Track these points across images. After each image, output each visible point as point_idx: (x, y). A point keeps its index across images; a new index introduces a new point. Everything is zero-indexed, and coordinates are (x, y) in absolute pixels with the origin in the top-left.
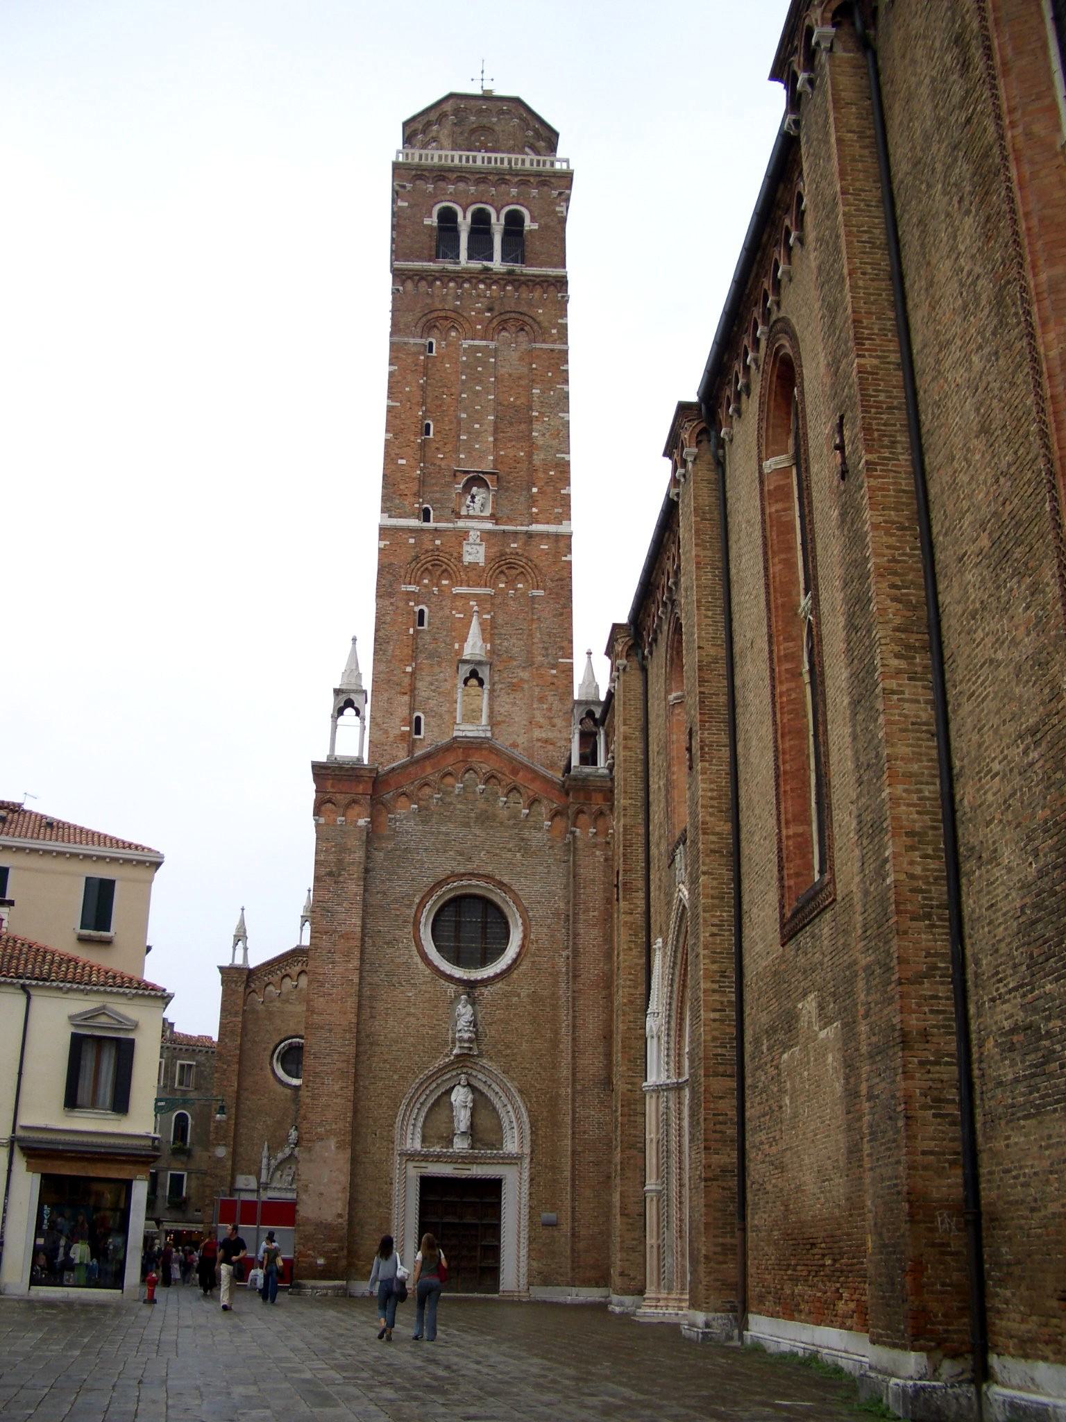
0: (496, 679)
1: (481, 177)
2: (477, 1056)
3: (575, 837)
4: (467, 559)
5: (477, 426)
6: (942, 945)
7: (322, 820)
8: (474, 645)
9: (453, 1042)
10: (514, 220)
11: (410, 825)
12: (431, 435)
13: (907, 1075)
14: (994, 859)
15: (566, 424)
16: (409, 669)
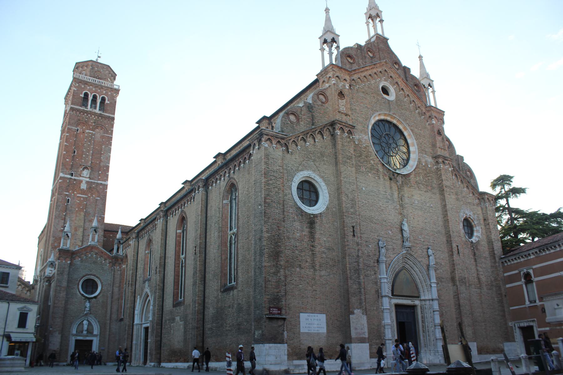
0: (86, 218)
1: (96, 86)
2: (90, 314)
3: (114, 268)
4: (82, 187)
5: (88, 153)
6: (202, 317)
7: (60, 261)
8: (95, 224)
9: (85, 311)
10: (103, 99)
11: (79, 263)
12: (76, 154)
13: (197, 332)
14: (209, 309)
15: (110, 156)
16: (64, 214)
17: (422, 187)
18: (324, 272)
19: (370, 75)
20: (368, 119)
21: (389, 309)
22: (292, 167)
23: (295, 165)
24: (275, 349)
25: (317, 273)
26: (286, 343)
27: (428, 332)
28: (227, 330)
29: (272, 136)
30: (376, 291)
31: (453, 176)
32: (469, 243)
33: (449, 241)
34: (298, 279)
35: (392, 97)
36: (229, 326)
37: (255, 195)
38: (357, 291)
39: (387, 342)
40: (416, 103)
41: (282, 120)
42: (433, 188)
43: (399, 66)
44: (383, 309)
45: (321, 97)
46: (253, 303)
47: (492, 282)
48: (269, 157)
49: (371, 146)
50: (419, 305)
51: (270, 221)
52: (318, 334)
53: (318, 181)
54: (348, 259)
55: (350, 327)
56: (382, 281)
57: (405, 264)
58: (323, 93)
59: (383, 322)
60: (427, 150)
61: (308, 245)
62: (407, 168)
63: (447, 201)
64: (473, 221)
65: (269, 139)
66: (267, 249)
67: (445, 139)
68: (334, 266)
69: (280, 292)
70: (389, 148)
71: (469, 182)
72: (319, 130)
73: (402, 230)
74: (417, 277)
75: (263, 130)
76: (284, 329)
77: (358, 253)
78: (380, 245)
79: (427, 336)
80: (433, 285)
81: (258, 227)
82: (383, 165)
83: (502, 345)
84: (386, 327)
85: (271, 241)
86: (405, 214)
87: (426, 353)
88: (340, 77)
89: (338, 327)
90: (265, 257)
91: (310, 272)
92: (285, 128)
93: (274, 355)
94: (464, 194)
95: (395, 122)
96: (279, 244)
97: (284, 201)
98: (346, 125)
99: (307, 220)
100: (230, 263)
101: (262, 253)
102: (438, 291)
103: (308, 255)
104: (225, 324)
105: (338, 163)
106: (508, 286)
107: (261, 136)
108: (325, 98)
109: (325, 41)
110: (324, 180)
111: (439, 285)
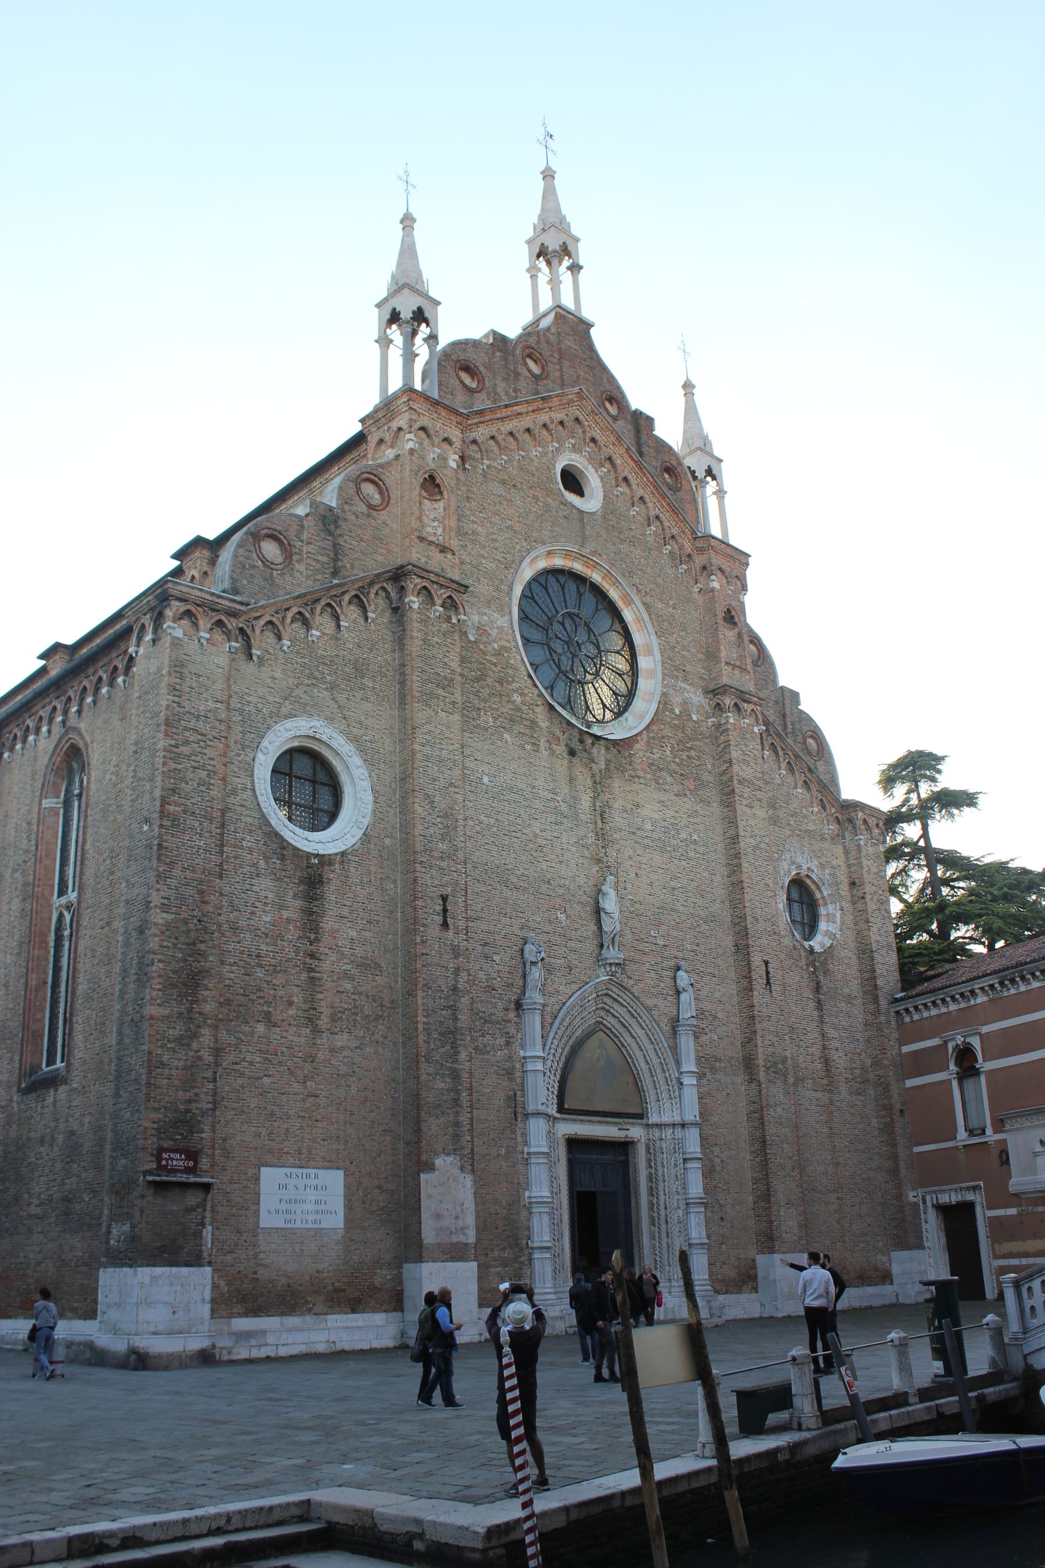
17: (669, 779)
18: (345, 1036)
19: (528, 430)
20: (512, 565)
21: (547, 1154)
22: (260, 706)
23: (271, 699)
24: (171, 1284)
25: (323, 1040)
26: (210, 1264)
27: (667, 1223)
28: (30, 1216)
29: (198, 605)
30: (509, 1098)
31: (763, 749)
32: (803, 953)
33: (742, 949)
34: (258, 1059)
35: (592, 502)
36: (38, 1202)
37: (133, 789)
38: (445, 1098)
39: (537, 1255)
40: (666, 524)
41: (235, 556)
42: (702, 784)
43: (619, 409)
44: (529, 1154)
45: (368, 489)
46: (109, 1135)
47: (863, 1068)
48: (185, 671)
49: (517, 647)
51: (177, 872)
52: (318, 1233)
53: (340, 750)
54: (423, 998)
55: (418, 1210)
56: (530, 1067)
57: (602, 1013)
58: (373, 478)
59: (527, 1194)
60: (688, 668)
61: (297, 951)
62: (627, 719)
63: (741, 824)
64: (819, 888)
65: (188, 613)
66: (160, 961)
67: (746, 639)
68: (378, 1018)
69: (196, 1101)
70: (574, 656)
71: (810, 770)
72: (353, 593)
73: (598, 911)
74: (639, 1055)
75: (170, 585)
76: (204, 1217)
77: (456, 981)
78: (526, 955)
79: (664, 1234)
80: (689, 1080)
81: (136, 892)
82: (552, 708)
83: (884, 1259)
85: (176, 938)
86: (612, 862)
88: (432, 432)
89: (382, 1209)
90: (154, 990)
91: (297, 1038)
92: (245, 582)
93: (165, 1303)
94: (795, 805)
95: (596, 577)
96: (202, 946)
97: (223, 812)
98: (442, 581)
99: (299, 874)
100: (52, 998)
101: (146, 974)
102: (700, 1098)
103: (296, 982)
104: (26, 1196)
105: (408, 697)
106: (910, 1083)
107: (163, 601)
108: (381, 493)
109: (394, 318)
110: (362, 751)
111: (704, 1081)
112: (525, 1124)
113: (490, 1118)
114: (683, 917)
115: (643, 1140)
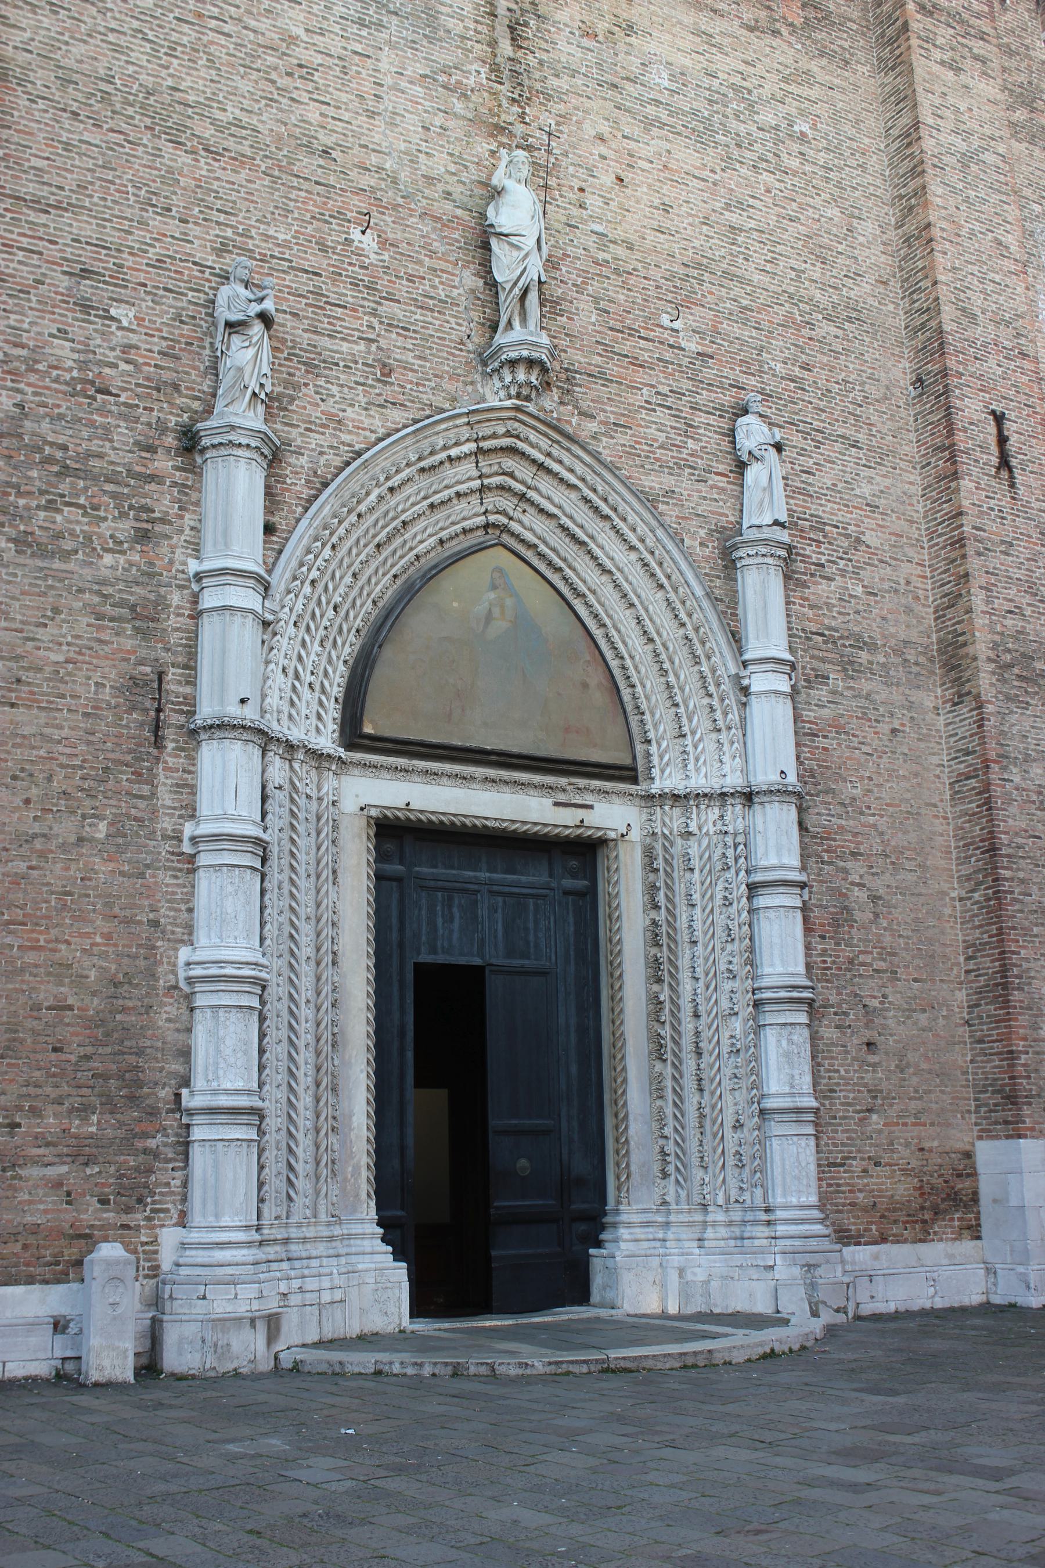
27: (699, 1054)
39: (197, 1134)
50: (635, 835)
79: (689, 1084)
80: (760, 682)
84: (200, 1001)
87: (667, 1224)
111: (821, 693)
112: (192, 759)
113: (56, 734)
114: (763, 298)
115: (635, 835)
